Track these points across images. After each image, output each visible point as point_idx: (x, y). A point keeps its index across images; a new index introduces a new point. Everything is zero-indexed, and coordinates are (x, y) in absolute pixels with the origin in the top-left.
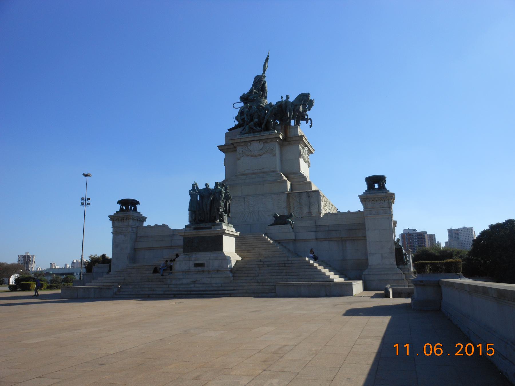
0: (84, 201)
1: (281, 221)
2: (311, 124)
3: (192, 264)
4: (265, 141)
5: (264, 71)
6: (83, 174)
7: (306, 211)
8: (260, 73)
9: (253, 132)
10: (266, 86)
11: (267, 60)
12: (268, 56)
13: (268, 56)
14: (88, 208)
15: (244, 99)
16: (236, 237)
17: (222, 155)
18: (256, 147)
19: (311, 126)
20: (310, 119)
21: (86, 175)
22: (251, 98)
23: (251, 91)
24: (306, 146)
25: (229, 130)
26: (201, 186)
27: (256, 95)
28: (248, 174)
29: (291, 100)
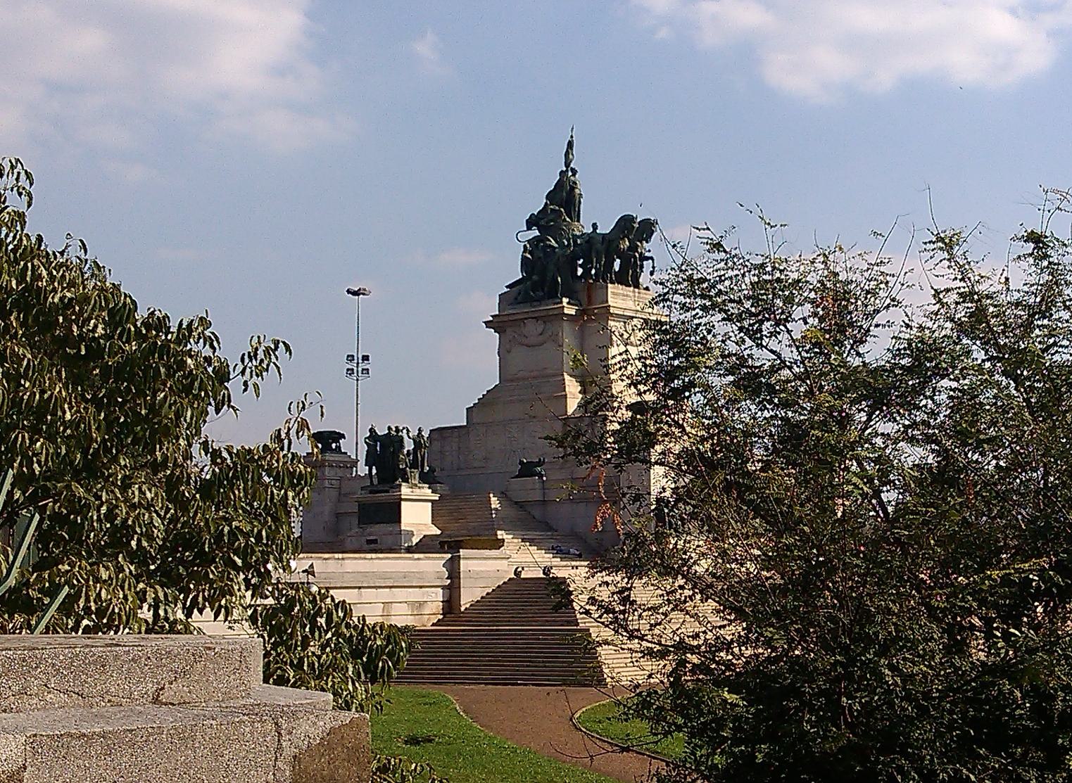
0: (353, 365)
1: (527, 470)
2: (653, 267)
3: (363, 540)
5: (567, 165)
6: (348, 291)
8: (564, 169)
10: (577, 191)
11: (570, 145)
12: (572, 137)
13: (572, 137)
15: (530, 224)
18: (533, 329)
21: (356, 293)
22: (542, 223)
24: (632, 318)
25: (507, 287)
28: (524, 379)
29: (605, 228)
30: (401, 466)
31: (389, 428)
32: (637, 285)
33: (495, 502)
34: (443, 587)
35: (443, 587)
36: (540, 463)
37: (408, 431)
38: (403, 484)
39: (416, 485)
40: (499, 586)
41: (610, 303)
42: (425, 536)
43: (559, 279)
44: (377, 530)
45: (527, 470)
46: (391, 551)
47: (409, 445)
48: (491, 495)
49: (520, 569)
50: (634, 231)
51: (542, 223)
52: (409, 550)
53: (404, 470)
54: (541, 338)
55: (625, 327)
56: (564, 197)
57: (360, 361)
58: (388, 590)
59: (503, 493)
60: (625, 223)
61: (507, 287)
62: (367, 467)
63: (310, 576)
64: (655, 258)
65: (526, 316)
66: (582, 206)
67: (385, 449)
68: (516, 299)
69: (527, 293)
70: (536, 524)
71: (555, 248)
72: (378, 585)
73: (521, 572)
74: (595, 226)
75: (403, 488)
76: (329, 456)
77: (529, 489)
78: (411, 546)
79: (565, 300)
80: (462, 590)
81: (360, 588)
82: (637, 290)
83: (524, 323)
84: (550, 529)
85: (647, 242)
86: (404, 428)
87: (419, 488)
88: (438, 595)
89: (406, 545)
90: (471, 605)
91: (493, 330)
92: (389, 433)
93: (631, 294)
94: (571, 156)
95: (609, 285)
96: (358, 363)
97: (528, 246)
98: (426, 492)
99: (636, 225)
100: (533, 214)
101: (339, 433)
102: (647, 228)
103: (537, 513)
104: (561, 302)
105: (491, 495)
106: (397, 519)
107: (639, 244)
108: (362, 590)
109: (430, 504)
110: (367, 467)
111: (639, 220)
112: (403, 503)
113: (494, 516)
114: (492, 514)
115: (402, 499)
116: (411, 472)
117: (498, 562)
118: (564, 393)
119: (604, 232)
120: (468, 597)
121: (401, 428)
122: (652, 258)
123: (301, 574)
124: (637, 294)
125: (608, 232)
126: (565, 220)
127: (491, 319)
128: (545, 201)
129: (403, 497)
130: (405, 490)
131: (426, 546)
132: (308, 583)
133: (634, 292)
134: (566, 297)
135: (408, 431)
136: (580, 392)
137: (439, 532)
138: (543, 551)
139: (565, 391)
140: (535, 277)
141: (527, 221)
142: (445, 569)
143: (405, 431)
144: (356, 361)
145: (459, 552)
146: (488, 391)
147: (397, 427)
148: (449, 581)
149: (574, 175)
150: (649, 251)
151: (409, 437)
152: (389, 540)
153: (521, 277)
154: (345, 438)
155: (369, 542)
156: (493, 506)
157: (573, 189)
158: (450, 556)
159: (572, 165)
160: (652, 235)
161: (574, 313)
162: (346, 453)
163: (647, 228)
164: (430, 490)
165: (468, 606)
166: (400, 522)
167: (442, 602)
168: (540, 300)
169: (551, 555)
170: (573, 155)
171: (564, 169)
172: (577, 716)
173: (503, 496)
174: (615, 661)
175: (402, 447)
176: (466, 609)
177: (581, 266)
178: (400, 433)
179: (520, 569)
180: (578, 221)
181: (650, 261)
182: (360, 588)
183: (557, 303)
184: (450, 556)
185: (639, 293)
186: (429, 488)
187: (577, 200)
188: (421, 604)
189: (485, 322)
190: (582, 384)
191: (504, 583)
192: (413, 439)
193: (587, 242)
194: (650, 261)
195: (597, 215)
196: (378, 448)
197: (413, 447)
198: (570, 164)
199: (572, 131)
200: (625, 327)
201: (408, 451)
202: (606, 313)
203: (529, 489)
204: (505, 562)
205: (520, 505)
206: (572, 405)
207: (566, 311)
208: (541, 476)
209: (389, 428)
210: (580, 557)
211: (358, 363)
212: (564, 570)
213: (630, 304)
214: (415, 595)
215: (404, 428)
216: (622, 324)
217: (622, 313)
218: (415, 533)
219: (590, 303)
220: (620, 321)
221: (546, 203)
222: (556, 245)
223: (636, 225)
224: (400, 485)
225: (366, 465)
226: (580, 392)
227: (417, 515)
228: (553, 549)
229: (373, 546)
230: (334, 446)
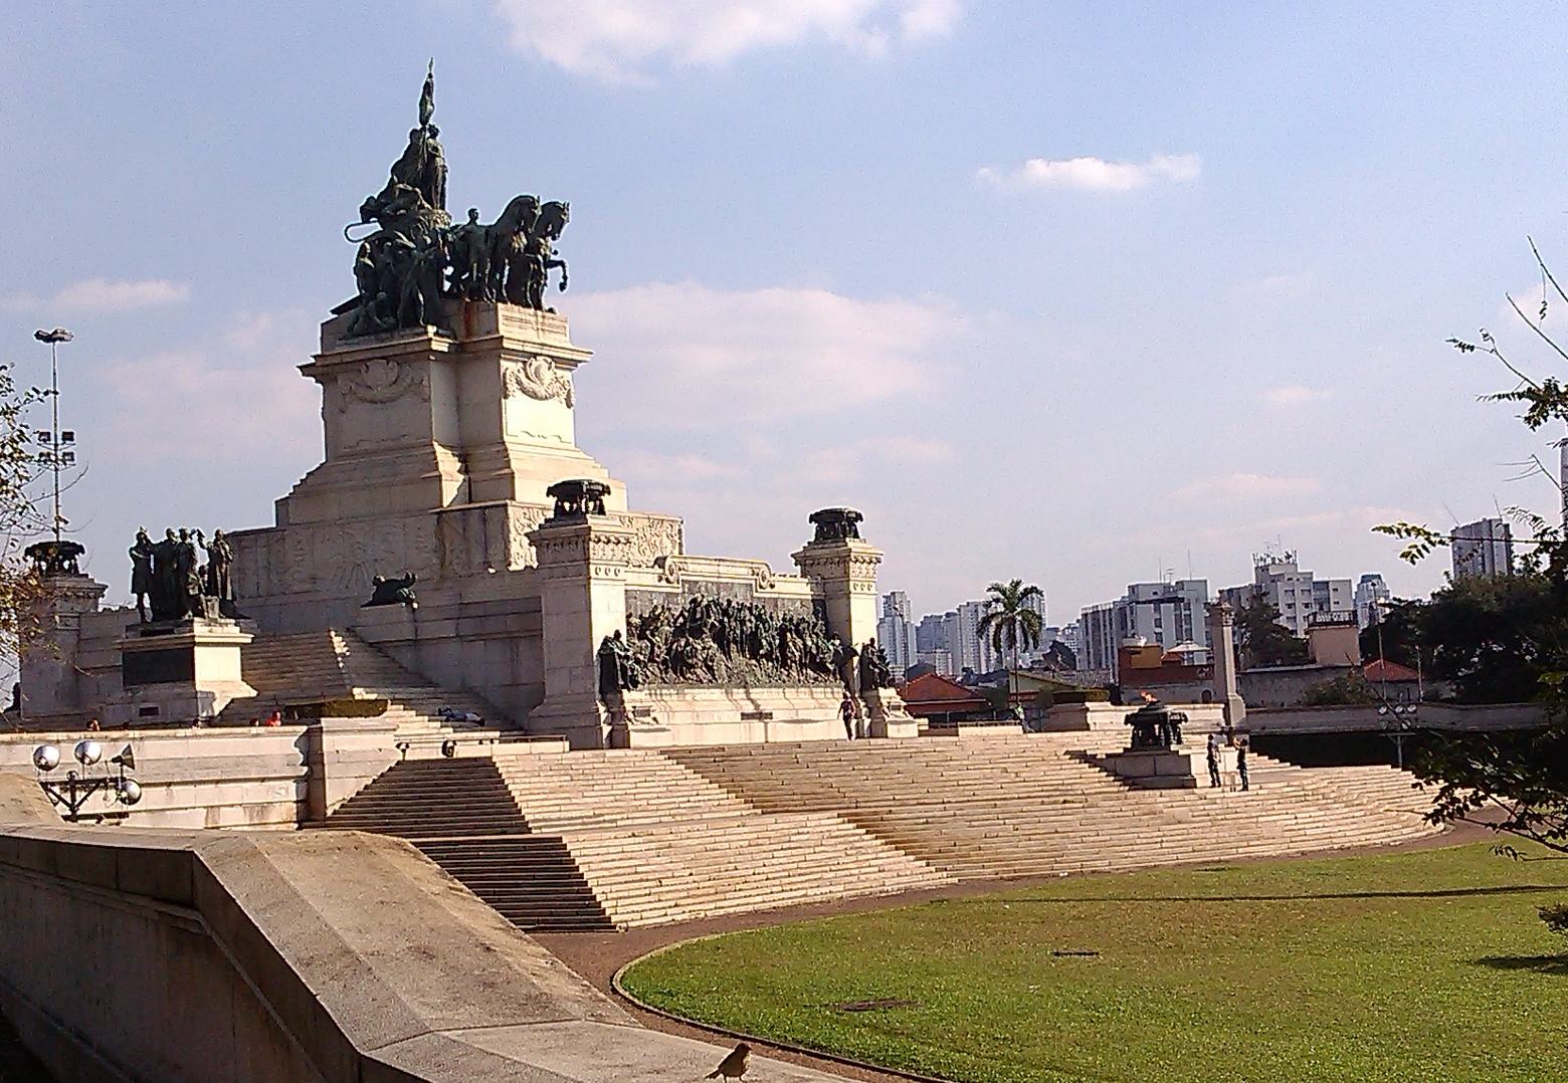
1: (387, 593)
2: (565, 278)
3: (135, 710)
4: (402, 359)
5: (424, 120)
6: (38, 336)
7: (478, 559)
9: (376, 333)
11: (428, 88)
12: (430, 76)
13: (430, 76)
14: (67, 473)
15: (368, 212)
16: (243, 646)
17: (314, 389)
18: (380, 375)
19: (563, 287)
20: (562, 264)
21: (49, 339)
22: (388, 210)
23: (392, 183)
24: (535, 355)
25: (333, 312)
26: (156, 538)
27: (401, 201)
28: (367, 453)
29: (489, 218)
30: (191, 592)
31: (169, 533)
32: (538, 307)
33: (339, 645)
34: (297, 779)
35: (297, 779)
36: (408, 582)
37: (200, 535)
38: (196, 619)
39: (215, 620)
40: (382, 775)
41: (502, 333)
42: (233, 701)
43: (421, 298)
44: (158, 693)
45: (387, 593)
46: (181, 725)
47: (202, 559)
48: (333, 634)
49: (450, 744)
50: (534, 219)
51: (388, 210)
52: (210, 722)
53: (196, 598)
54: (395, 389)
55: (525, 369)
56: (420, 171)
57: (60, 441)
58: (213, 786)
59: (348, 630)
60: (521, 208)
61: (333, 312)
62: (135, 595)
63: (125, 767)
64: (565, 261)
65: (370, 355)
66: (447, 186)
67: (164, 569)
68: (350, 329)
69: (368, 317)
70: (409, 675)
71: (413, 249)
72: (198, 778)
73: (452, 748)
74: (473, 214)
75: (195, 625)
76: (60, 581)
77: (392, 623)
78: (212, 717)
79: (432, 329)
80: (327, 781)
81: (169, 784)
82: (539, 313)
83: (367, 367)
84: (430, 684)
85: (554, 239)
86: (193, 532)
87: (221, 625)
88: (289, 792)
89: (204, 714)
90: (342, 806)
91: (313, 380)
92: (170, 539)
93: (533, 319)
94: (429, 107)
95: (500, 305)
96: (56, 445)
97: (368, 246)
98: (231, 630)
99: (539, 212)
100: (372, 198)
101: (74, 544)
102: (555, 216)
103: (406, 657)
104: (426, 333)
105: (333, 634)
106: (189, 675)
107: (542, 241)
108: (173, 788)
109: (238, 649)
110: (135, 595)
111: (541, 204)
112: (196, 649)
113: (341, 665)
114: (338, 662)
115: (195, 644)
116: (207, 601)
117: (379, 736)
118: (436, 473)
119: (486, 224)
120: (337, 792)
121: (189, 532)
122: (562, 264)
123: (110, 764)
124: (540, 320)
125: (493, 223)
126: (422, 207)
127: (313, 361)
128: (390, 176)
129: (197, 640)
130: (200, 629)
131: (236, 715)
132: (123, 779)
133: (536, 315)
134: (433, 325)
135: (200, 535)
136: (459, 471)
137: (254, 693)
138: (426, 718)
139: (437, 469)
140: (382, 295)
141: (362, 208)
142: (297, 750)
143: (195, 536)
144: (53, 442)
145: (319, 722)
146: (308, 474)
147: (182, 531)
148: (306, 769)
149: (434, 136)
150: (556, 253)
151: (202, 546)
152: (177, 707)
153: (358, 294)
154: (83, 553)
155: (144, 712)
156: (338, 651)
157: (433, 157)
158: (305, 728)
159: (431, 122)
160: (561, 227)
161: (446, 350)
162: (87, 575)
163: (555, 216)
164: (238, 628)
165: (337, 807)
166: (192, 677)
167: (297, 802)
168: (391, 330)
169: (439, 724)
170: (432, 105)
171: (419, 127)
172: (618, 977)
173: (350, 633)
174: (614, 888)
175: (193, 561)
176: (335, 812)
177: (448, 278)
178: (188, 541)
179: (450, 744)
180: (443, 208)
181: (560, 268)
182: (169, 784)
183: (419, 335)
184: (305, 728)
185: (543, 317)
186: (236, 625)
187: (440, 177)
188: (264, 807)
189: (300, 368)
190: (464, 458)
191: (391, 769)
192: (209, 550)
193: (462, 238)
194: (560, 268)
195: (473, 197)
196: (152, 564)
197: (208, 560)
198: (428, 118)
199: (430, 66)
200: (525, 369)
201: (202, 567)
202: (497, 348)
203: (392, 623)
204: (390, 736)
205: (378, 647)
206: (451, 491)
207: (435, 346)
208: (409, 602)
209: (169, 533)
210: (481, 725)
211: (56, 445)
212: (470, 746)
213: (530, 334)
214: (254, 793)
215: (193, 532)
216: (521, 365)
217: (521, 348)
218: (217, 695)
219: (469, 334)
220: (517, 361)
221: (392, 179)
222: (412, 245)
223: (539, 212)
224: (192, 621)
225: (133, 592)
226: (459, 471)
227: (219, 667)
228: (440, 715)
229: (151, 719)
230: (66, 564)
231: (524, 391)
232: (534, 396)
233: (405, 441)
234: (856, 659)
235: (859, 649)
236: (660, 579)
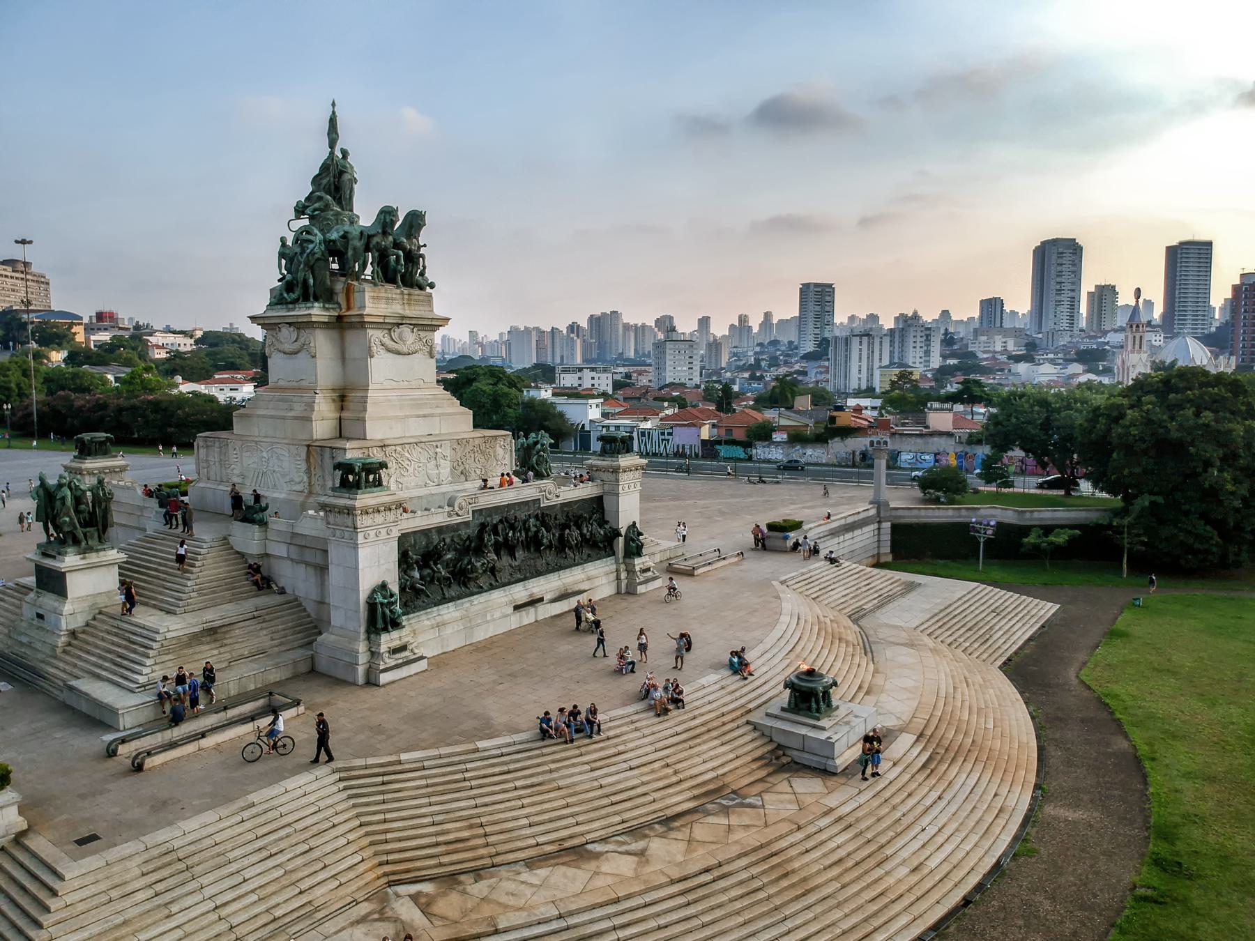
5: (332, 145)
11: (333, 121)
12: (334, 113)
13: (334, 113)
15: (300, 211)
56: (333, 182)
102: (415, 221)
163: (415, 221)
168: (295, 302)
189: (251, 318)
231: (389, 350)
232: (398, 353)
233: (304, 383)
234: (621, 539)
235: (623, 532)
236: (450, 516)
